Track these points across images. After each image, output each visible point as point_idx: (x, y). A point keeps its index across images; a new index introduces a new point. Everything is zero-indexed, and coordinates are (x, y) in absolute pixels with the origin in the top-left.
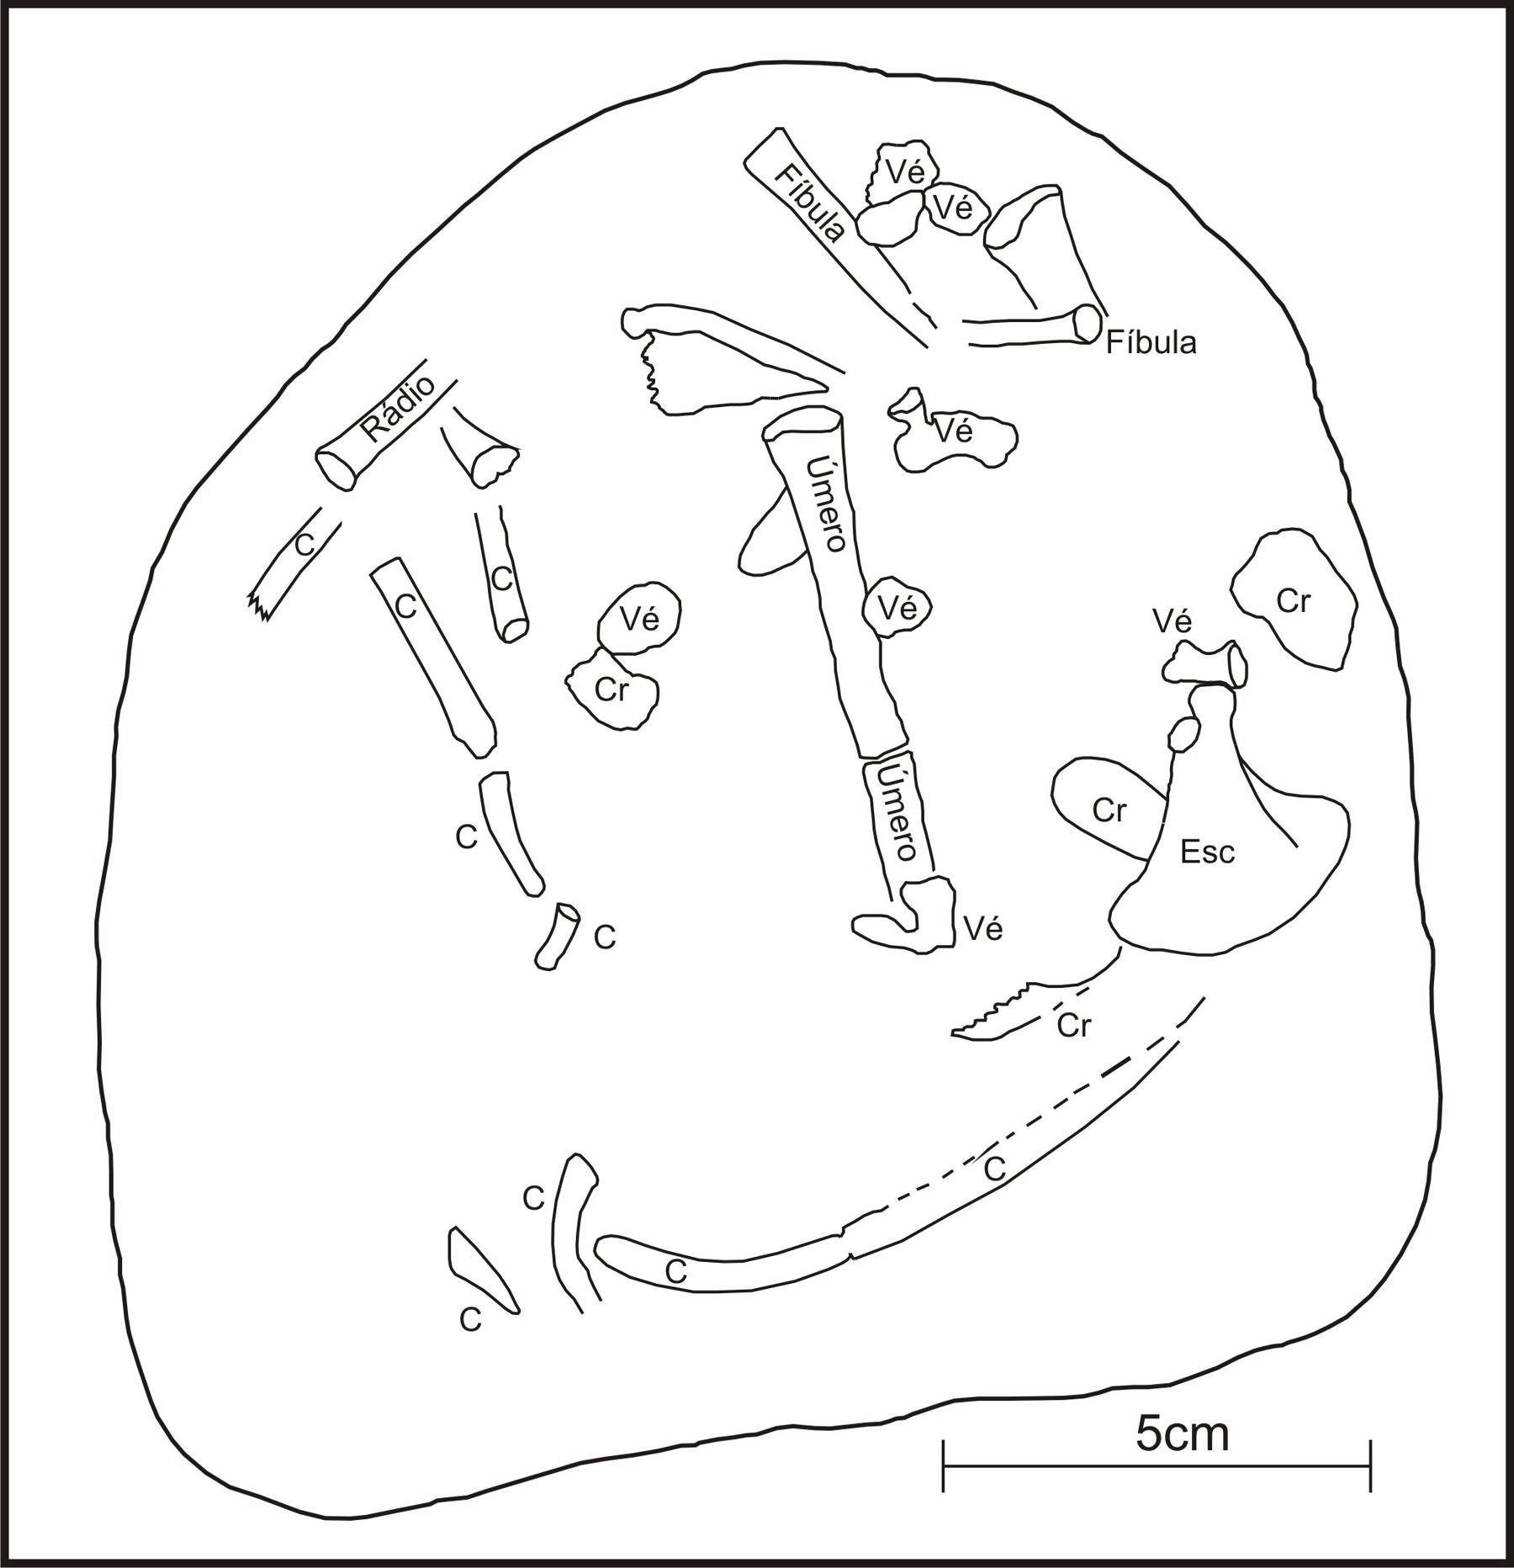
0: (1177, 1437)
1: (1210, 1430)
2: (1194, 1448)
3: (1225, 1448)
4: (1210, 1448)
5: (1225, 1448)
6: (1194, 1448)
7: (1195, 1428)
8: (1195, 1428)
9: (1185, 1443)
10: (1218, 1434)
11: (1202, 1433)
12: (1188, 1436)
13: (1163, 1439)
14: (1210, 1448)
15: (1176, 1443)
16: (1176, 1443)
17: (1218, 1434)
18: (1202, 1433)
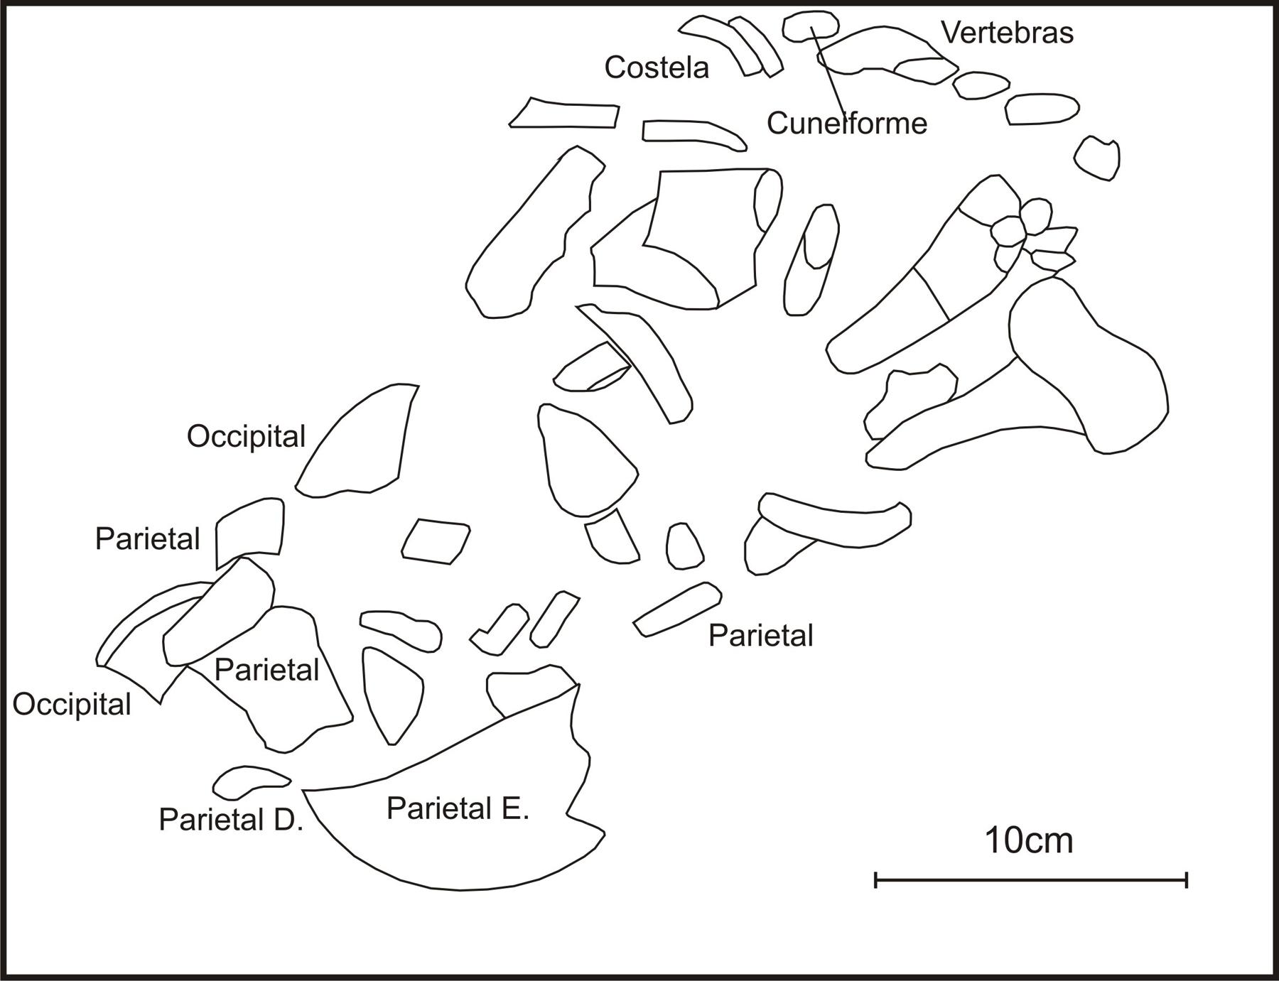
0: (1035, 843)
1: (1059, 838)
2: (1047, 851)
3: (1070, 851)
4: (1059, 851)
5: (1070, 851)
6: (1047, 851)
7: (1048, 837)
8: (1048, 837)
9: (1041, 848)
10: (1065, 840)
11: (1053, 840)
12: (1043, 843)
13: (1024, 842)
14: (1059, 851)
15: (1034, 846)
16: (1034, 846)
17: (1065, 840)
18: (1053, 840)
